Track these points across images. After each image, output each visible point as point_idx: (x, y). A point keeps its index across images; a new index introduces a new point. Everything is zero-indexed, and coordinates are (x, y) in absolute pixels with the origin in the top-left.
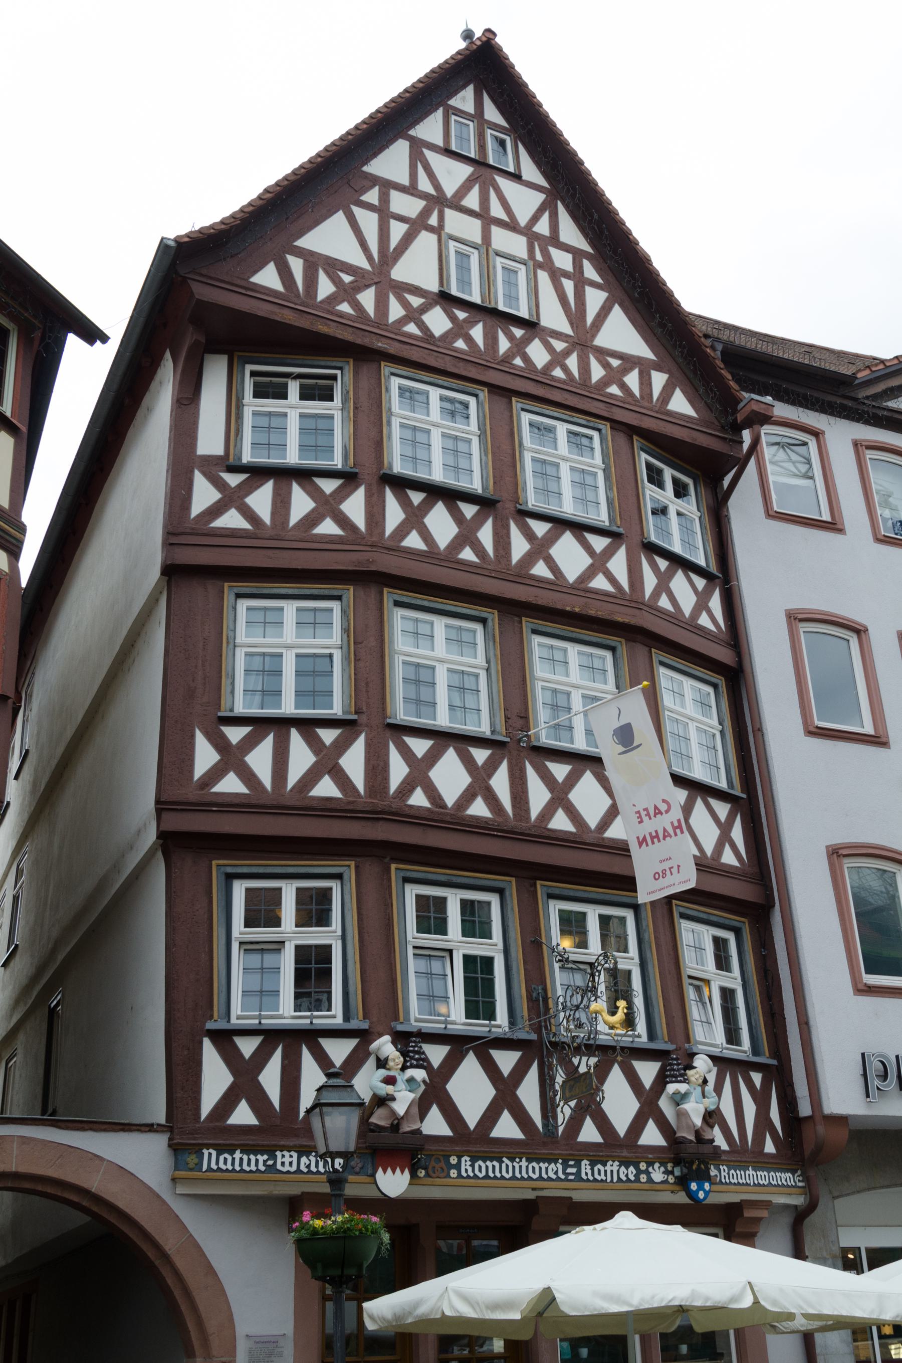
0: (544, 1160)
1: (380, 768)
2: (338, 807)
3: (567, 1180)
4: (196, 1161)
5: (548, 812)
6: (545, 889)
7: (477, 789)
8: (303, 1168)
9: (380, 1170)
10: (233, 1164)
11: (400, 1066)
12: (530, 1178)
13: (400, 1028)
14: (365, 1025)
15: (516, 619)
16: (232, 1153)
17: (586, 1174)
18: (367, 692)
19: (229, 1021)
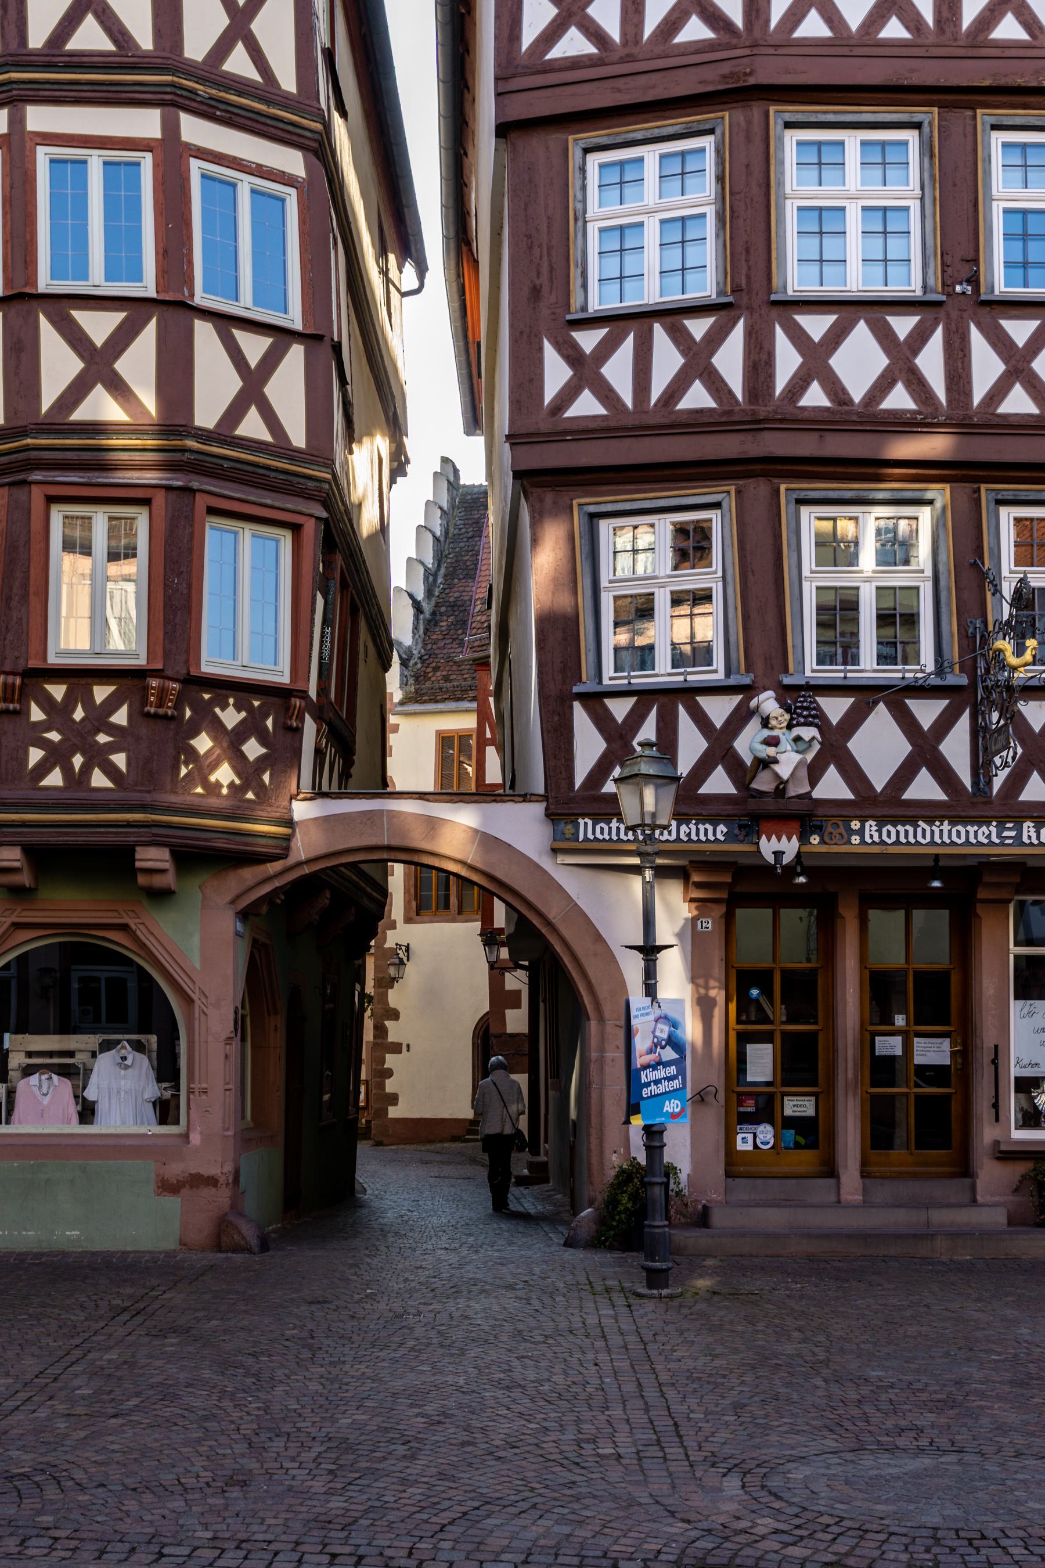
0: (972, 824)
1: (763, 363)
2: (712, 420)
3: (1003, 845)
4: (573, 831)
5: (999, 391)
6: (993, 494)
7: (897, 372)
8: (683, 837)
9: (764, 837)
10: (610, 833)
11: (785, 724)
12: (953, 843)
13: (787, 681)
14: (746, 680)
15: (969, 113)
16: (608, 823)
17: (1029, 837)
18: (747, 261)
19: (600, 682)
